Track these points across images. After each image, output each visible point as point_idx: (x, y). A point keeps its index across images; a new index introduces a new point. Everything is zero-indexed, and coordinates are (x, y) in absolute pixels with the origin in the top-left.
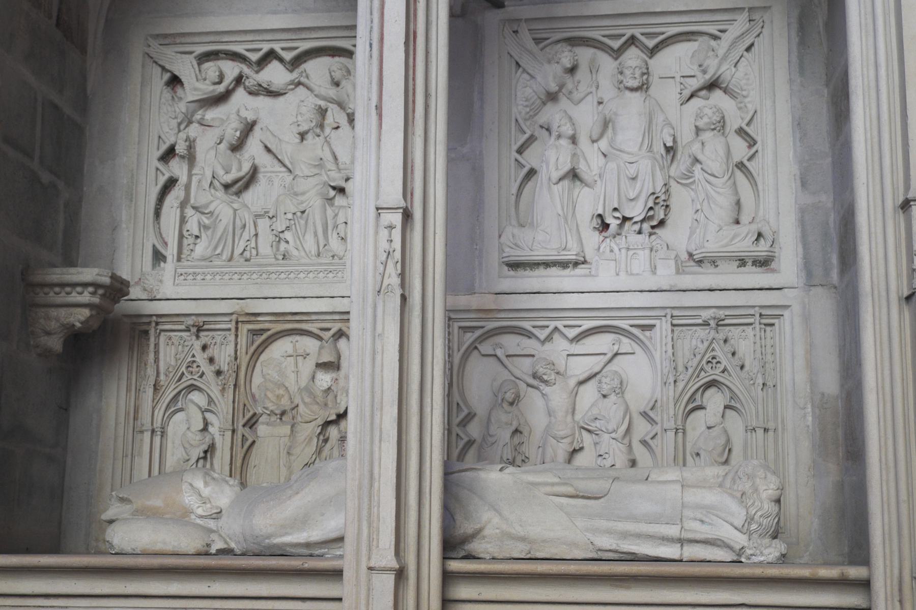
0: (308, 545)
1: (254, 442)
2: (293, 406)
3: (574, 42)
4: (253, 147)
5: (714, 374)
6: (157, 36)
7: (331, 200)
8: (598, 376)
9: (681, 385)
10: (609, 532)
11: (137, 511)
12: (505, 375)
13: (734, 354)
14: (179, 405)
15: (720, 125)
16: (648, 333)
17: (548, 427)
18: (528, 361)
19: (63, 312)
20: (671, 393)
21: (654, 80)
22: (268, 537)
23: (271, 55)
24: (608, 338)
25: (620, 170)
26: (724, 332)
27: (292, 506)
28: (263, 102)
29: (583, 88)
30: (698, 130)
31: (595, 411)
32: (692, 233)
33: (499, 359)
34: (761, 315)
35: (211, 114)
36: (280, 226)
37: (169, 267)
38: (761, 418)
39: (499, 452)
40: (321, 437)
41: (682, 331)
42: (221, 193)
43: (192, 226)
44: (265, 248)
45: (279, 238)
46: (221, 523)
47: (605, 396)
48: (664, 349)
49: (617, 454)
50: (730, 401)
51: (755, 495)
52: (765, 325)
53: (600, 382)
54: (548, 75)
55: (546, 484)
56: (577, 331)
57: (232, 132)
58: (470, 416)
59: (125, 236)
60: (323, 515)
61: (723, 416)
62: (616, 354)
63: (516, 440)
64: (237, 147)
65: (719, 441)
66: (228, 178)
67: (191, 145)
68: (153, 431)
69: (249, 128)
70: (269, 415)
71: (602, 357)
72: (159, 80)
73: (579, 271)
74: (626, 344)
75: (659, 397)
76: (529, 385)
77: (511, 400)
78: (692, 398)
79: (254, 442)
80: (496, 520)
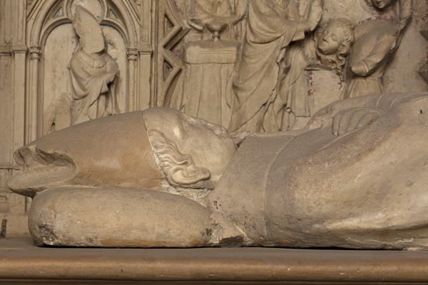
0: (385, 233)
1: (180, 71)
2: (236, 19)
11: (80, 176)
14: (61, 14)
22: (322, 219)
27: (364, 171)
40: (284, 65)
46: (213, 196)
60: (410, 184)
68: (27, 53)
70: (200, 31)
79: (180, 71)
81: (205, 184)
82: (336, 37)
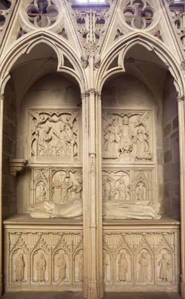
3: (114, 114)
4: (51, 133)
5: (141, 180)
6: (31, 109)
7: (67, 144)
10: (130, 215)
15: (142, 133)
17: (110, 189)
18: (106, 177)
19: (16, 168)
21: (129, 123)
23: (54, 114)
24: (121, 172)
25: (126, 142)
27: (69, 210)
28: (53, 123)
29: (116, 124)
30: (138, 133)
32: (137, 153)
35: (42, 126)
36: (57, 149)
37: (35, 157)
42: (45, 142)
43: (39, 149)
44: (54, 153)
45: (57, 151)
49: (123, 195)
54: (110, 121)
57: (47, 130)
59: (26, 151)
64: (48, 133)
66: (46, 139)
67: (38, 131)
69: (50, 129)
72: (31, 118)
73: (117, 160)
74: (125, 174)
80: (109, 213)
81: (52, 210)
82: (74, 187)
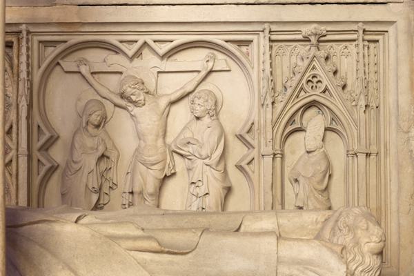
8: (191, 96)
9: (279, 107)
12: (91, 95)
13: (335, 73)
16: (244, 49)
18: (115, 78)
20: (269, 116)
24: (203, 53)
26: (326, 49)
31: (188, 135)
33: (84, 77)
34: (364, 31)
38: (363, 141)
39: (84, 180)
41: (281, 47)
47: (198, 118)
48: (262, 67)
50: (331, 123)
51: (356, 249)
52: (368, 41)
53: (193, 103)
55: (128, 238)
56: (169, 46)
58: (53, 140)
61: (323, 140)
62: (211, 72)
63: (103, 165)
65: (319, 168)
71: (195, 74)
74: (221, 61)
75: (256, 119)
76: (116, 105)
77: (96, 123)
78: (291, 120)
